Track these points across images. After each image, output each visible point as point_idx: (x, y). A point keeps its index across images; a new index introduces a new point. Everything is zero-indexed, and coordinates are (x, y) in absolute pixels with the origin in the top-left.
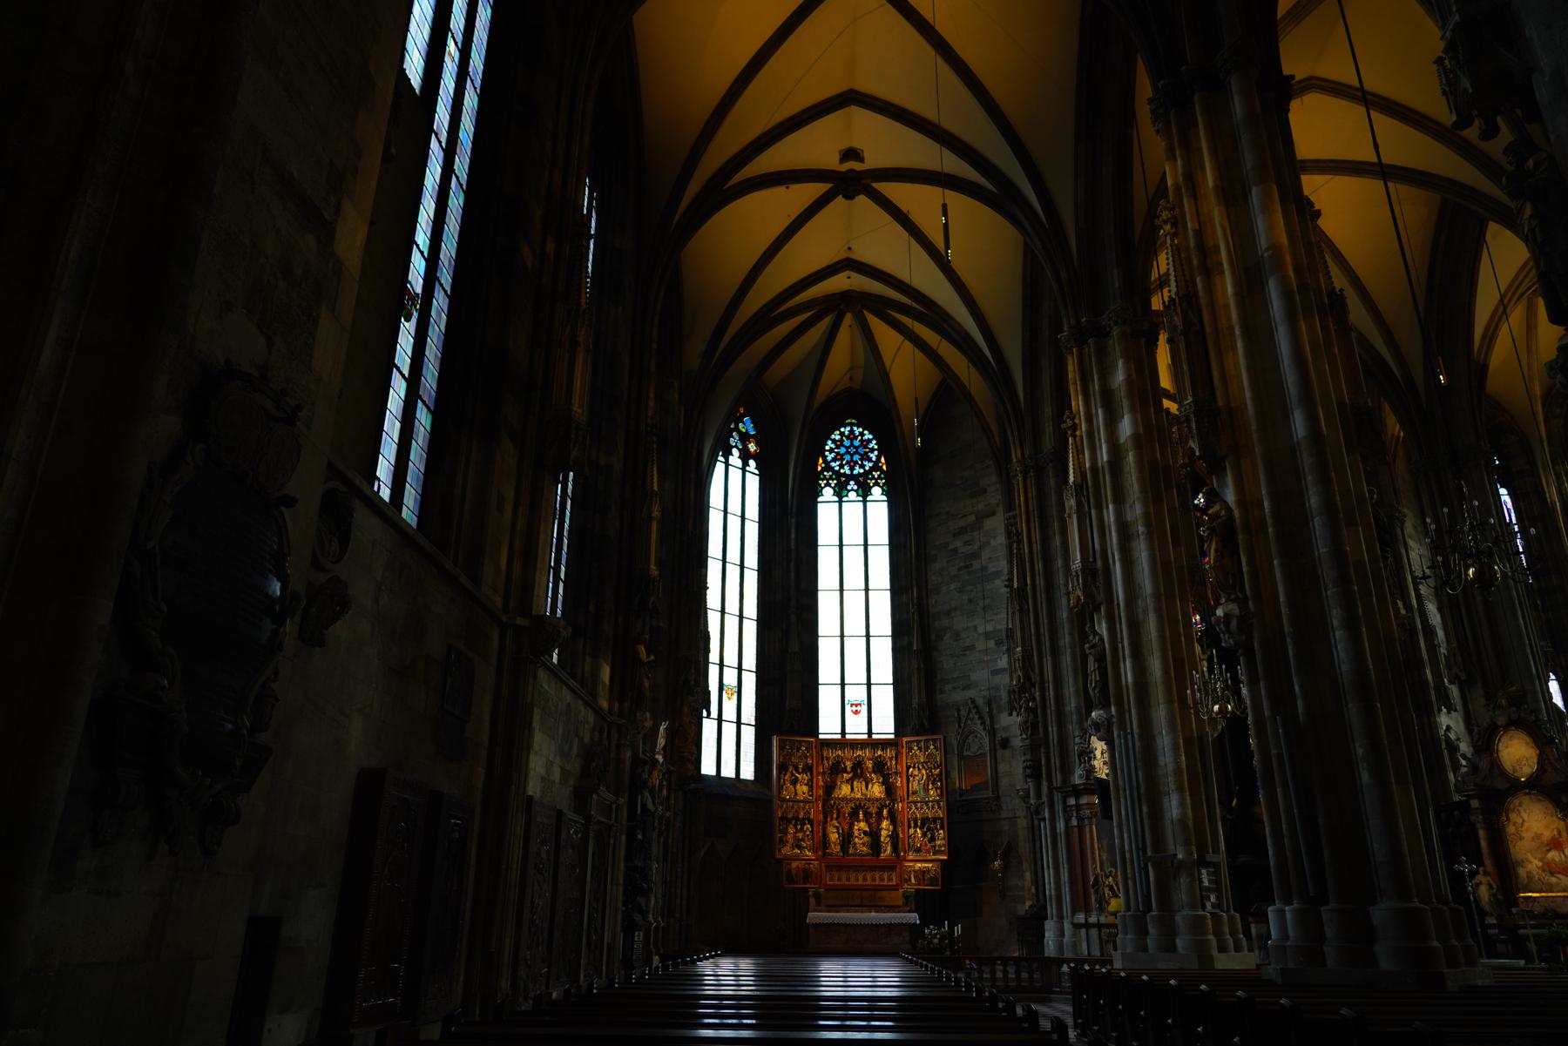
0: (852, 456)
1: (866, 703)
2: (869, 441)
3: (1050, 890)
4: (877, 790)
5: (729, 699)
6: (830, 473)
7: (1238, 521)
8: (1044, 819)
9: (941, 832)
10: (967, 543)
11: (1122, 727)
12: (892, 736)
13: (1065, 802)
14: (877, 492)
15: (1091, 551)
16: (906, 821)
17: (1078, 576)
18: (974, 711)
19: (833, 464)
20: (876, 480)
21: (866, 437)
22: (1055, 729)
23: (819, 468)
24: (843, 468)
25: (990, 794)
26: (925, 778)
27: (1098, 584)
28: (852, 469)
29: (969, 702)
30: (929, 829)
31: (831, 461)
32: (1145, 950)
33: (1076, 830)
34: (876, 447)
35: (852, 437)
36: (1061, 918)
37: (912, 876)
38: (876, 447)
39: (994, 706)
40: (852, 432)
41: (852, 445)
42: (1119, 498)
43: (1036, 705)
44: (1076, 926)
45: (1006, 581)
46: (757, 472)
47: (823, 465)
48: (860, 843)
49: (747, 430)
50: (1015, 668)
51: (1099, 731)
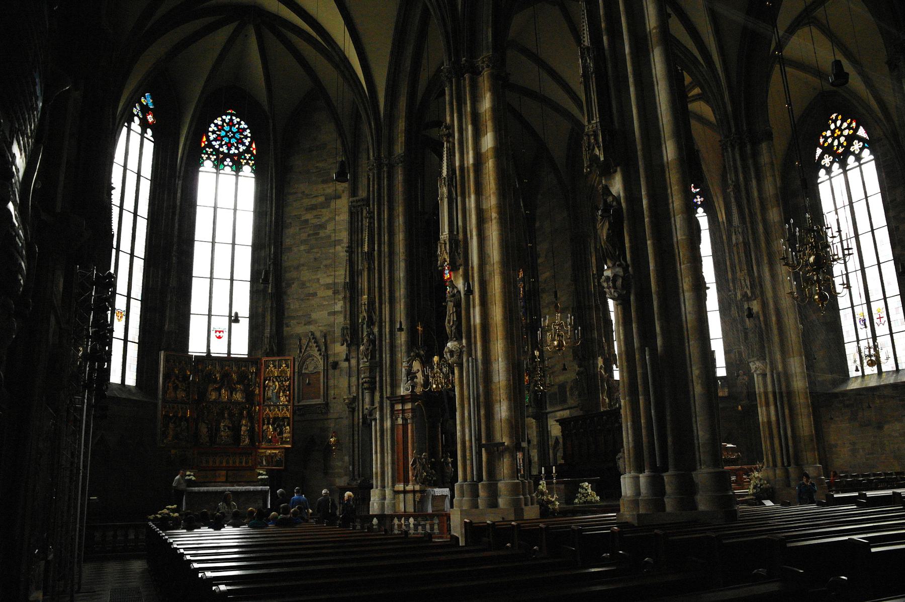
0: (230, 139)
1: (227, 330)
2: (244, 130)
3: (376, 468)
4: (238, 396)
5: (119, 320)
6: (211, 150)
7: (625, 211)
8: (375, 420)
9: (288, 427)
10: (317, 217)
11: (469, 354)
12: (247, 356)
13: (392, 406)
14: (247, 170)
15: (455, 227)
16: (261, 419)
17: (445, 244)
18: (313, 341)
19: (214, 143)
20: (247, 160)
21: (242, 126)
22: (388, 356)
23: (203, 145)
24: (222, 147)
25: (320, 401)
26: (277, 387)
27: (459, 251)
28: (229, 149)
29: (310, 334)
30: (278, 426)
31: (212, 141)
32: (477, 507)
33: (401, 427)
34: (249, 135)
35: (231, 124)
36: (383, 487)
37: (264, 460)
38: (249, 135)
39: (328, 338)
40: (231, 120)
41: (230, 130)
42: (479, 192)
43: (375, 338)
44: (397, 493)
45: (347, 247)
46: (152, 139)
47: (206, 143)
48: (224, 433)
49: (147, 104)
50: (361, 311)
51: (453, 357)
